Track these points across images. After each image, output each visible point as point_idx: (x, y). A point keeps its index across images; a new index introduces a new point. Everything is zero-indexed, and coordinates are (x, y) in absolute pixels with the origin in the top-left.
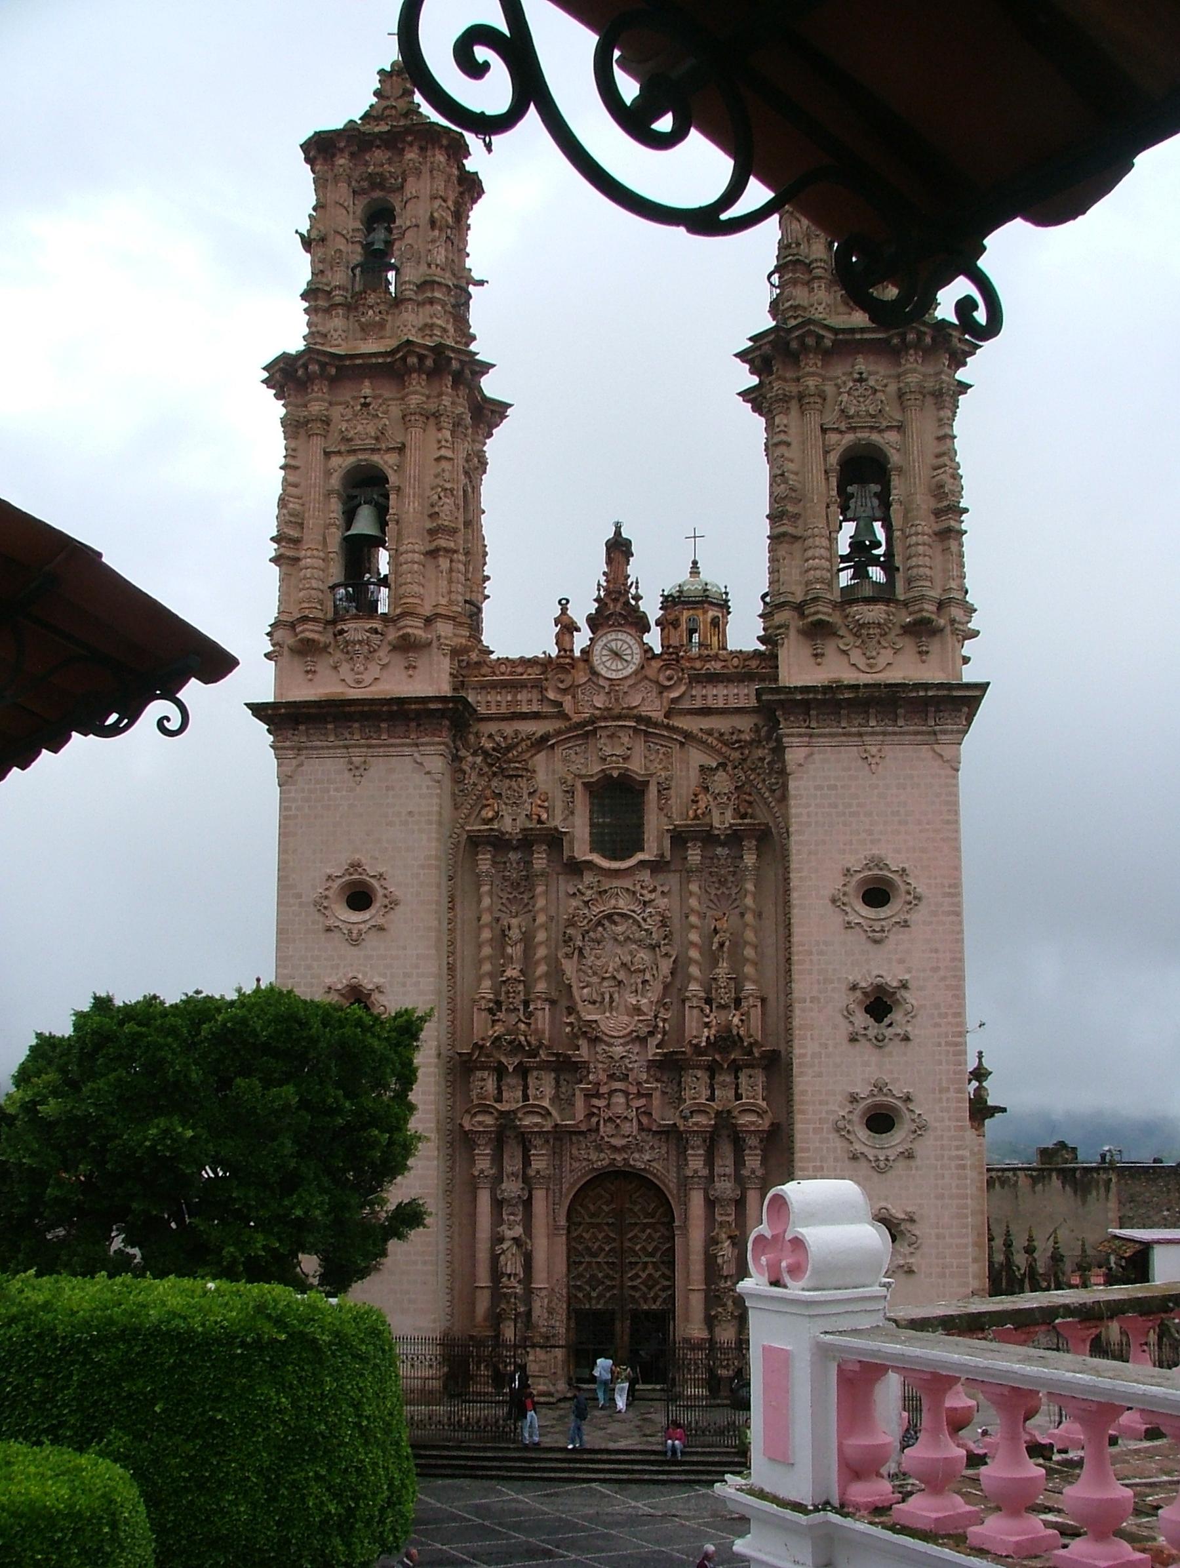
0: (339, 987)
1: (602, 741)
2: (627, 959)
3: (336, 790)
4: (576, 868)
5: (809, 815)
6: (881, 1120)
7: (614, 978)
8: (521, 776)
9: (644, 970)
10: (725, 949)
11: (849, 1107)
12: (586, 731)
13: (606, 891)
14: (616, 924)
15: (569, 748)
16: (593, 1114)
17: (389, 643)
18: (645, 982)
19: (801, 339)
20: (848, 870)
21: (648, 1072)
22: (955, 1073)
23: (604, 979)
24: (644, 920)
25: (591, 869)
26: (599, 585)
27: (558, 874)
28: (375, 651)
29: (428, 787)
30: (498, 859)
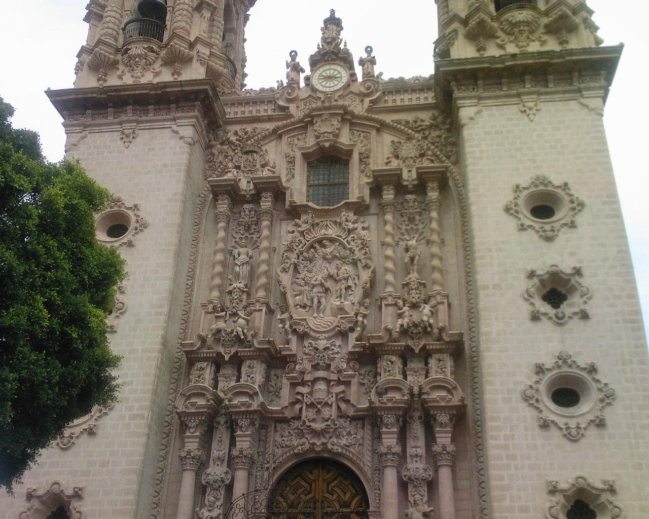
1: (318, 124)
2: (333, 271)
3: (110, 152)
4: (294, 212)
5: (481, 151)
6: (566, 394)
7: (322, 285)
8: (256, 152)
9: (348, 277)
10: (415, 262)
11: (535, 378)
12: (306, 123)
13: (317, 224)
14: (324, 246)
15: (293, 136)
16: (298, 401)
17: (162, 60)
18: (348, 288)
20: (518, 187)
21: (348, 363)
22: (636, 347)
23: (314, 286)
24: (349, 243)
25: (306, 213)
26: (319, 45)
27: (281, 220)
28: (150, 64)
29: (180, 148)
30: (235, 210)
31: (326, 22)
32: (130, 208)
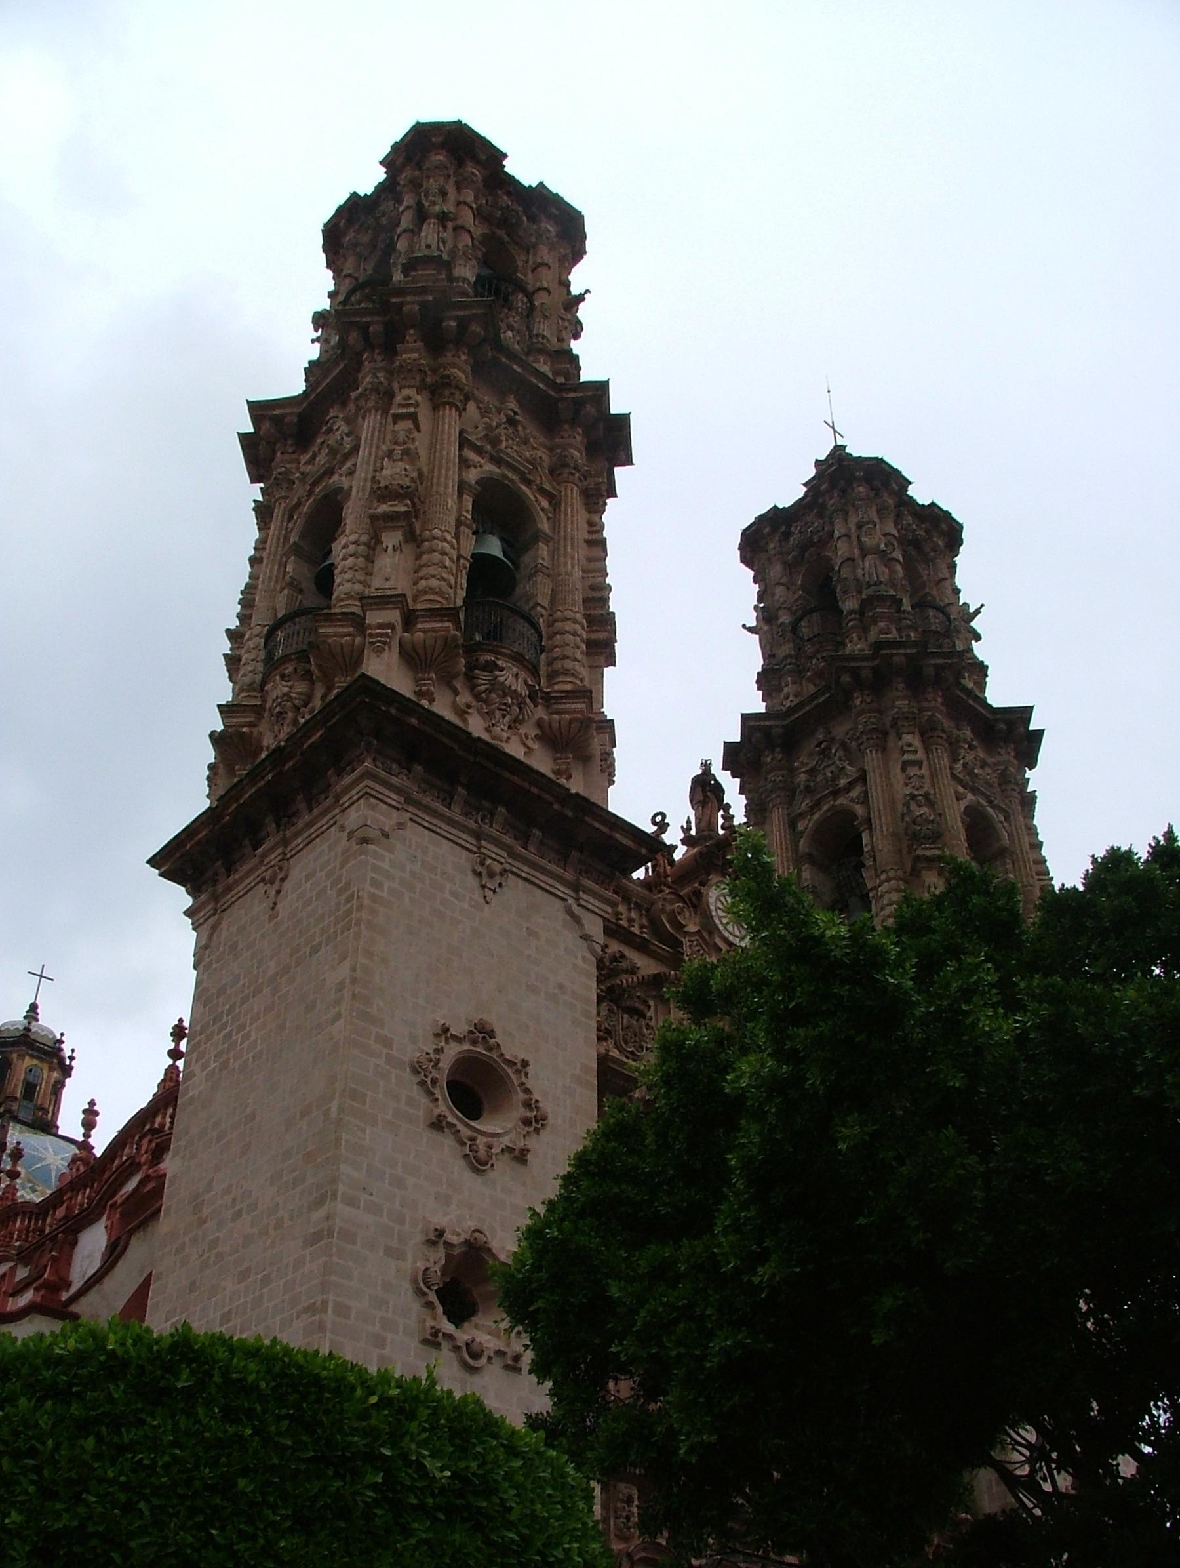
0: (454, 1240)
3: (454, 894)
19: (938, 668)
32: (511, 1063)
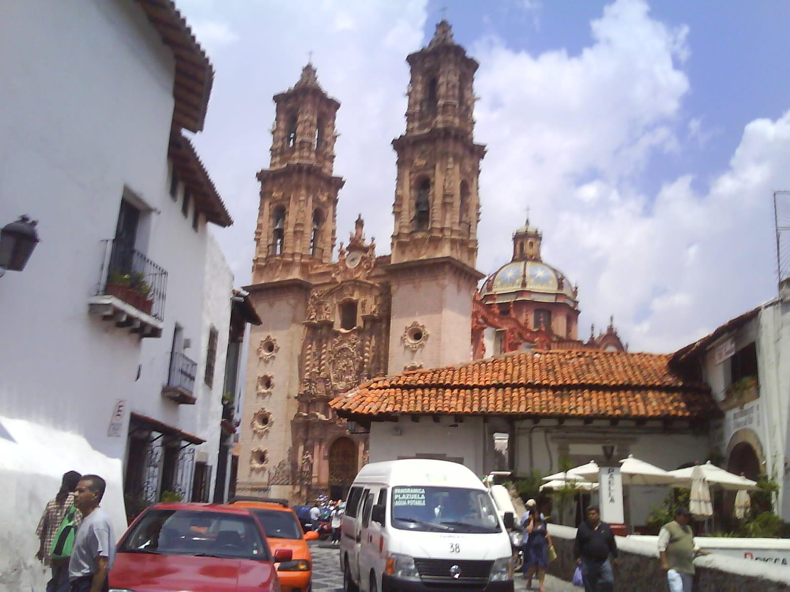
4: (337, 334)
31: (357, 222)
